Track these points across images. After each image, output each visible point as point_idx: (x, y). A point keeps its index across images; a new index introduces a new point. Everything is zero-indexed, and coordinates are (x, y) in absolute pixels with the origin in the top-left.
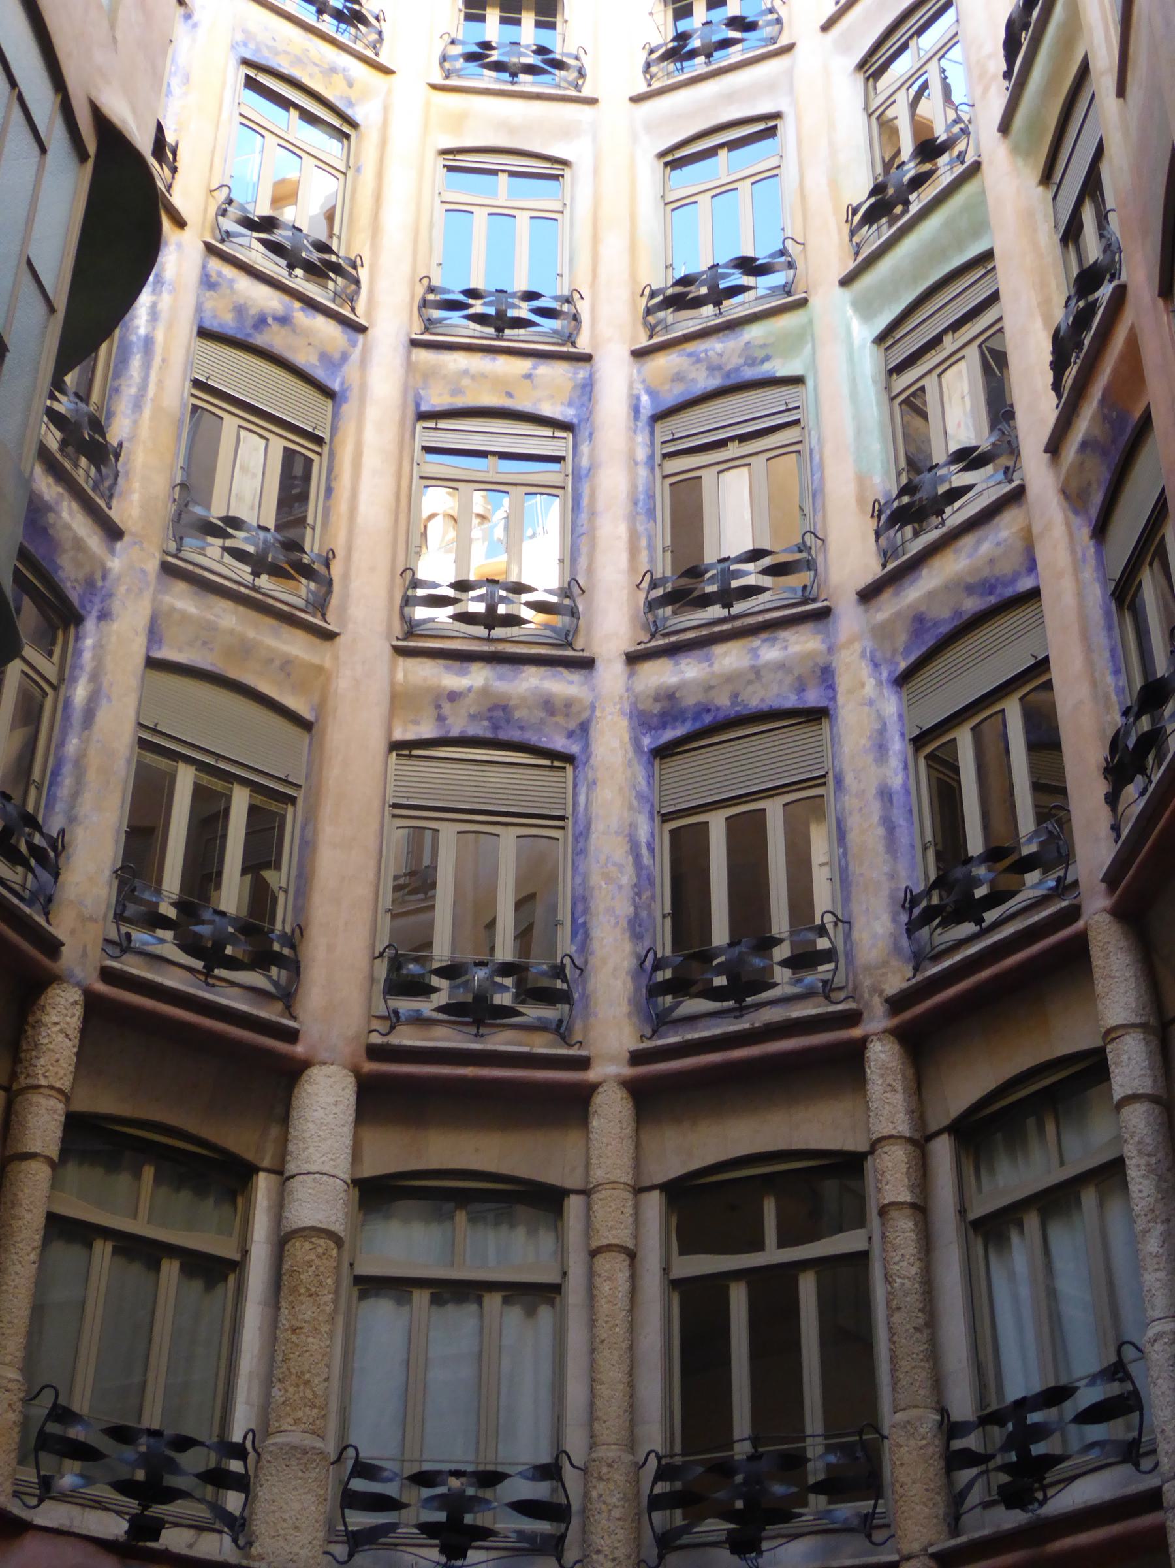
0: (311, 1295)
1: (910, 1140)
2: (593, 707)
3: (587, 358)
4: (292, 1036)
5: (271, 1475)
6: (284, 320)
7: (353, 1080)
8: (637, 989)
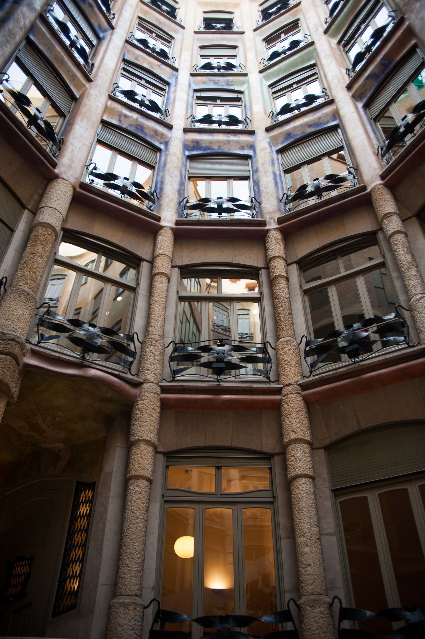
0: (43, 245)
5: (11, 298)
7: (72, 189)
8: (179, 208)
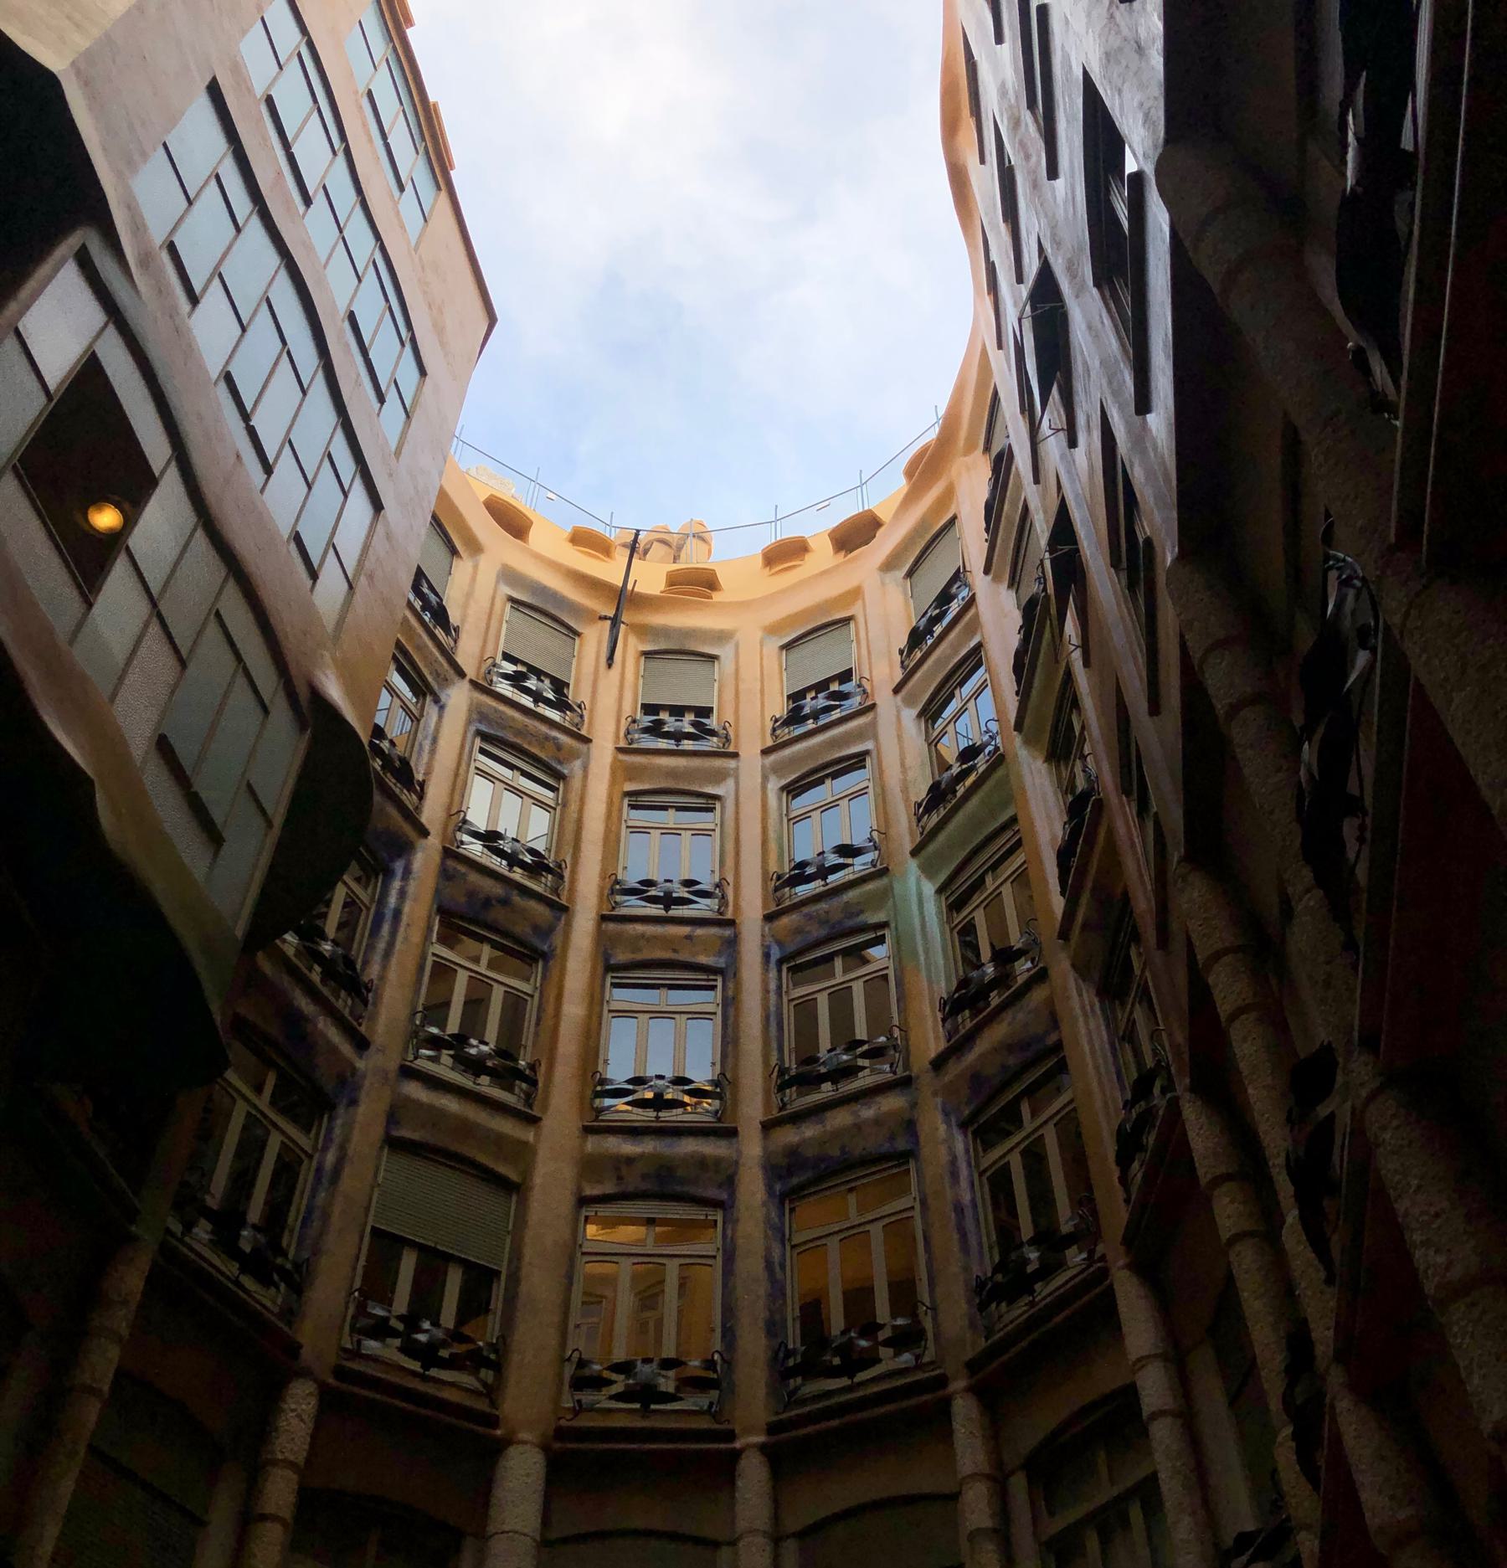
1: (988, 1477)
2: (737, 1162)
3: (731, 923)
4: (493, 1422)
6: (505, 902)
